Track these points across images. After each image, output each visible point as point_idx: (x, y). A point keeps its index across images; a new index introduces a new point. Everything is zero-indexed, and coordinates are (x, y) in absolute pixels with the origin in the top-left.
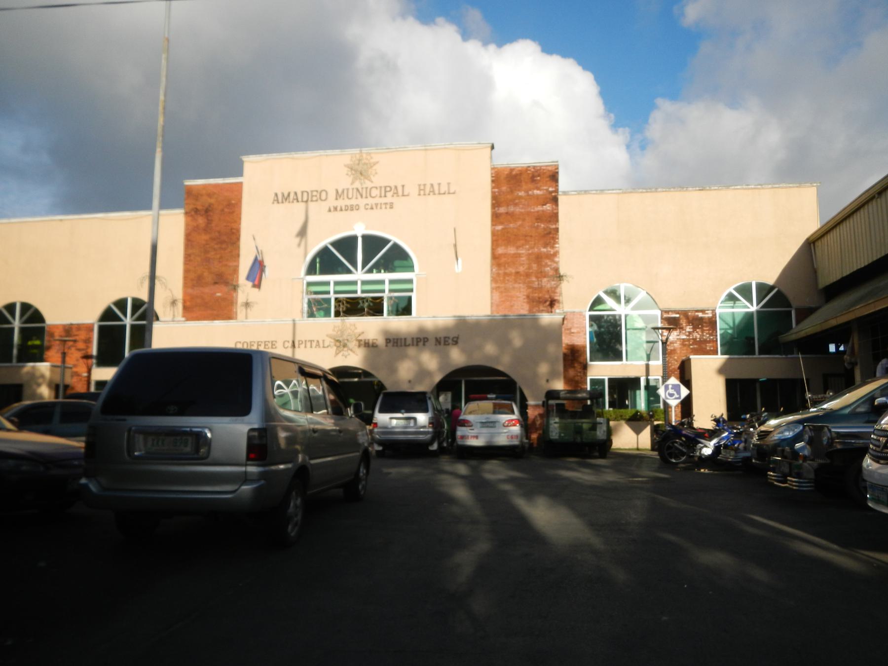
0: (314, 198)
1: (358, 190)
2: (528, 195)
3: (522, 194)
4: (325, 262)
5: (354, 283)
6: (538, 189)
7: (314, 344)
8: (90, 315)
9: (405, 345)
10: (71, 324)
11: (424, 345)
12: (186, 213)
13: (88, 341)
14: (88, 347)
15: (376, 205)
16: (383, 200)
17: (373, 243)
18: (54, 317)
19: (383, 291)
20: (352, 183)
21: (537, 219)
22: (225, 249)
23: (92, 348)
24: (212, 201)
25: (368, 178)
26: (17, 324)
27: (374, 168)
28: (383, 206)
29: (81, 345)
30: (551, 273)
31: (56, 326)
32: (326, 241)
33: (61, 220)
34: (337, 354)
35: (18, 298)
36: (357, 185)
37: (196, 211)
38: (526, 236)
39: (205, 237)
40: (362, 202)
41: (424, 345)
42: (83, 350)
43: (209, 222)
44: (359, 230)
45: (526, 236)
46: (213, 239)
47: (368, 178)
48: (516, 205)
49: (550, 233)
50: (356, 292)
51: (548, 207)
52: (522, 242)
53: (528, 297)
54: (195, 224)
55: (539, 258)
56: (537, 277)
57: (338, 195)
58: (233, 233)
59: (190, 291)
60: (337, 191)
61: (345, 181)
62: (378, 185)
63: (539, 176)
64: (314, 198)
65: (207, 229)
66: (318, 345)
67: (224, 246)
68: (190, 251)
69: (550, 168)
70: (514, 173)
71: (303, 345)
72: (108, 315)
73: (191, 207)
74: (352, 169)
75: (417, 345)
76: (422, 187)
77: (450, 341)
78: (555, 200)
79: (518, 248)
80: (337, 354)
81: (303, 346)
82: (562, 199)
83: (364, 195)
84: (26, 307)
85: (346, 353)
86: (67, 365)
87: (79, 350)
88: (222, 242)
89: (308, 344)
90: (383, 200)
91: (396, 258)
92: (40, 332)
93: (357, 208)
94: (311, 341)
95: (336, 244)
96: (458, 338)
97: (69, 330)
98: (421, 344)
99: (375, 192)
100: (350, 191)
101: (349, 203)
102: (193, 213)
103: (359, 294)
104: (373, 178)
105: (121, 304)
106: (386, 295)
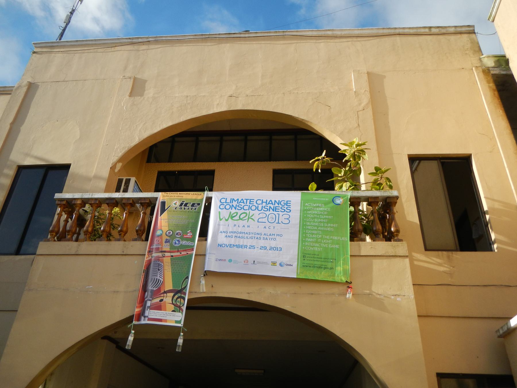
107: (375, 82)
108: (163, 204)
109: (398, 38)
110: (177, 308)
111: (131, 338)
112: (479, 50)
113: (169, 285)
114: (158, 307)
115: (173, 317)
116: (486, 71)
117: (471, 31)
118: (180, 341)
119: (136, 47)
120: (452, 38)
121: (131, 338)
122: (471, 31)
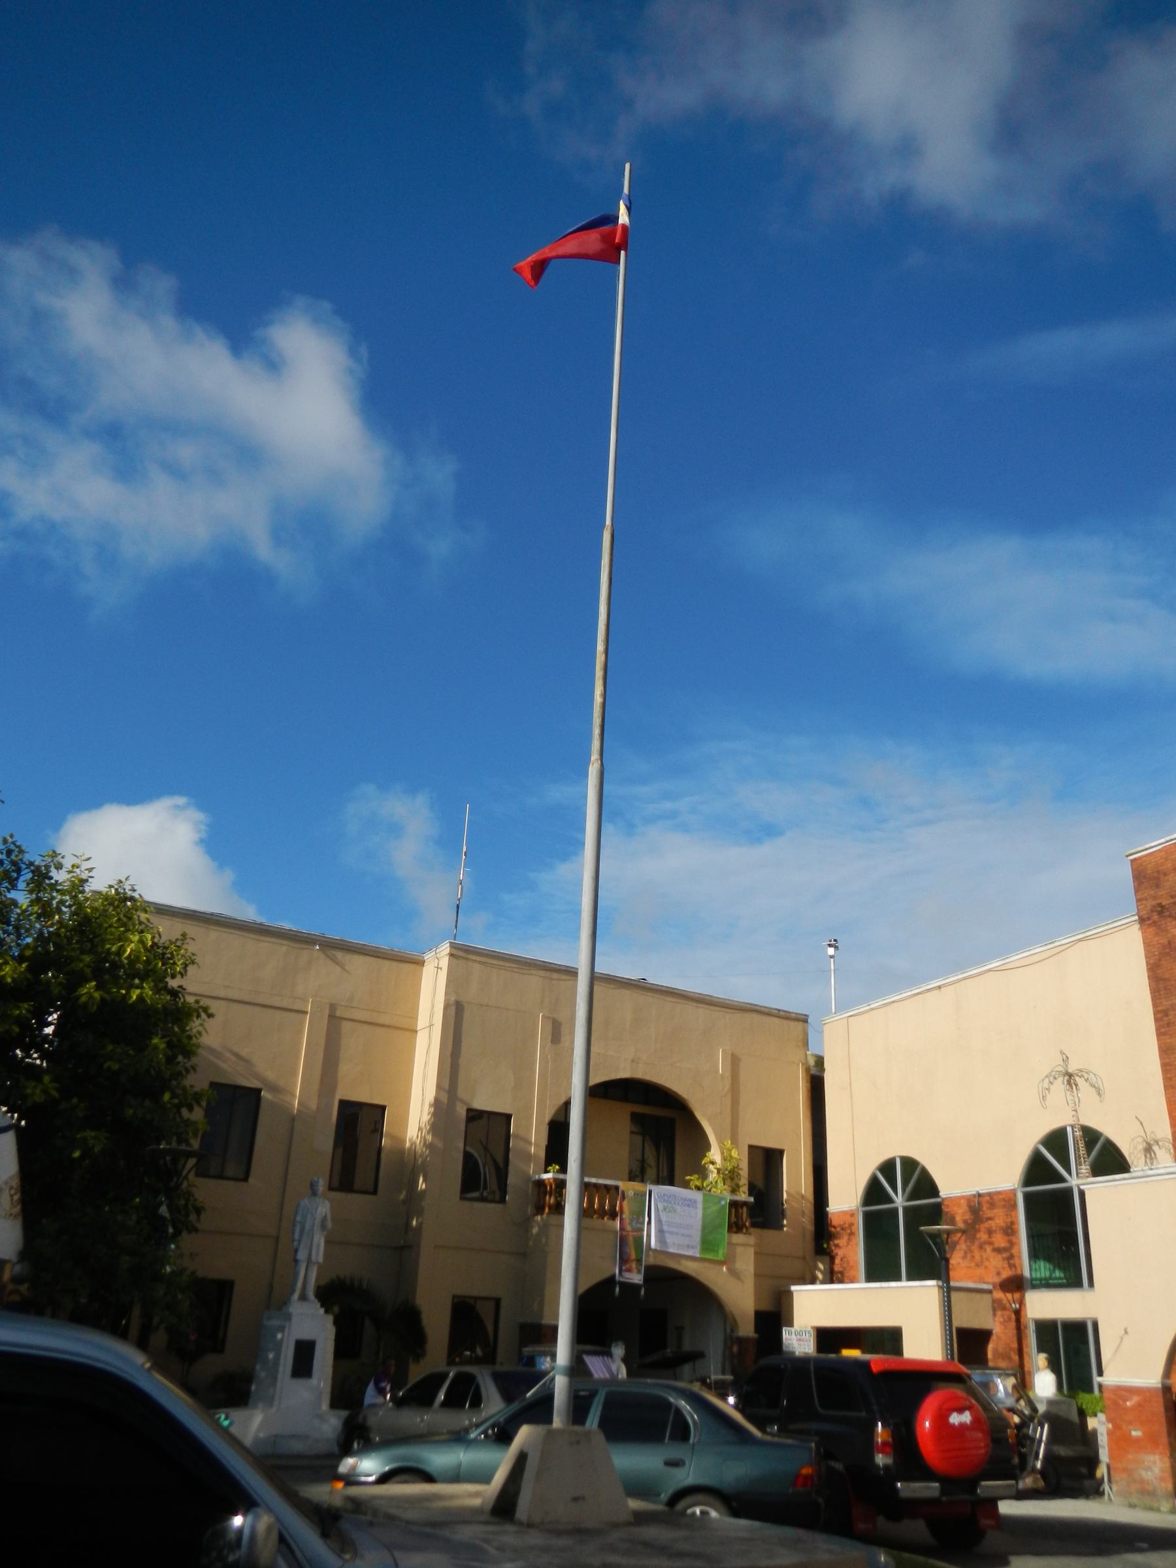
8: (1007, 1175)
10: (980, 1195)
12: (1142, 920)
13: (1010, 1230)
14: (1012, 1244)
18: (952, 1185)
23: (1019, 1244)
26: (899, 1201)
29: (1000, 1240)
31: (955, 1200)
33: (939, 987)
35: (896, 1150)
37: (1161, 910)
42: (1005, 1250)
54: (1164, 941)
68: (1166, 1004)
72: (1037, 1170)
73: (1150, 903)
84: (910, 1164)
86: (952, 1284)
87: (998, 1250)
92: (936, 1213)
97: (979, 1205)
102: (1156, 917)
105: (1056, 1141)
107: (735, 1062)
108: (623, 1193)
109: (755, 1016)
110: (639, 1272)
111: (617, 1290)
112: (806, 1044)
113: (633, 1256)
114: (629, 1270)
115: (637, 1278)
116: (807, 1070)
117: (806, 1021)
118: (643, 1292)
119: (548, 974)
120: (793, 1024)
121: (617, 1290)
122: (804, 1019)
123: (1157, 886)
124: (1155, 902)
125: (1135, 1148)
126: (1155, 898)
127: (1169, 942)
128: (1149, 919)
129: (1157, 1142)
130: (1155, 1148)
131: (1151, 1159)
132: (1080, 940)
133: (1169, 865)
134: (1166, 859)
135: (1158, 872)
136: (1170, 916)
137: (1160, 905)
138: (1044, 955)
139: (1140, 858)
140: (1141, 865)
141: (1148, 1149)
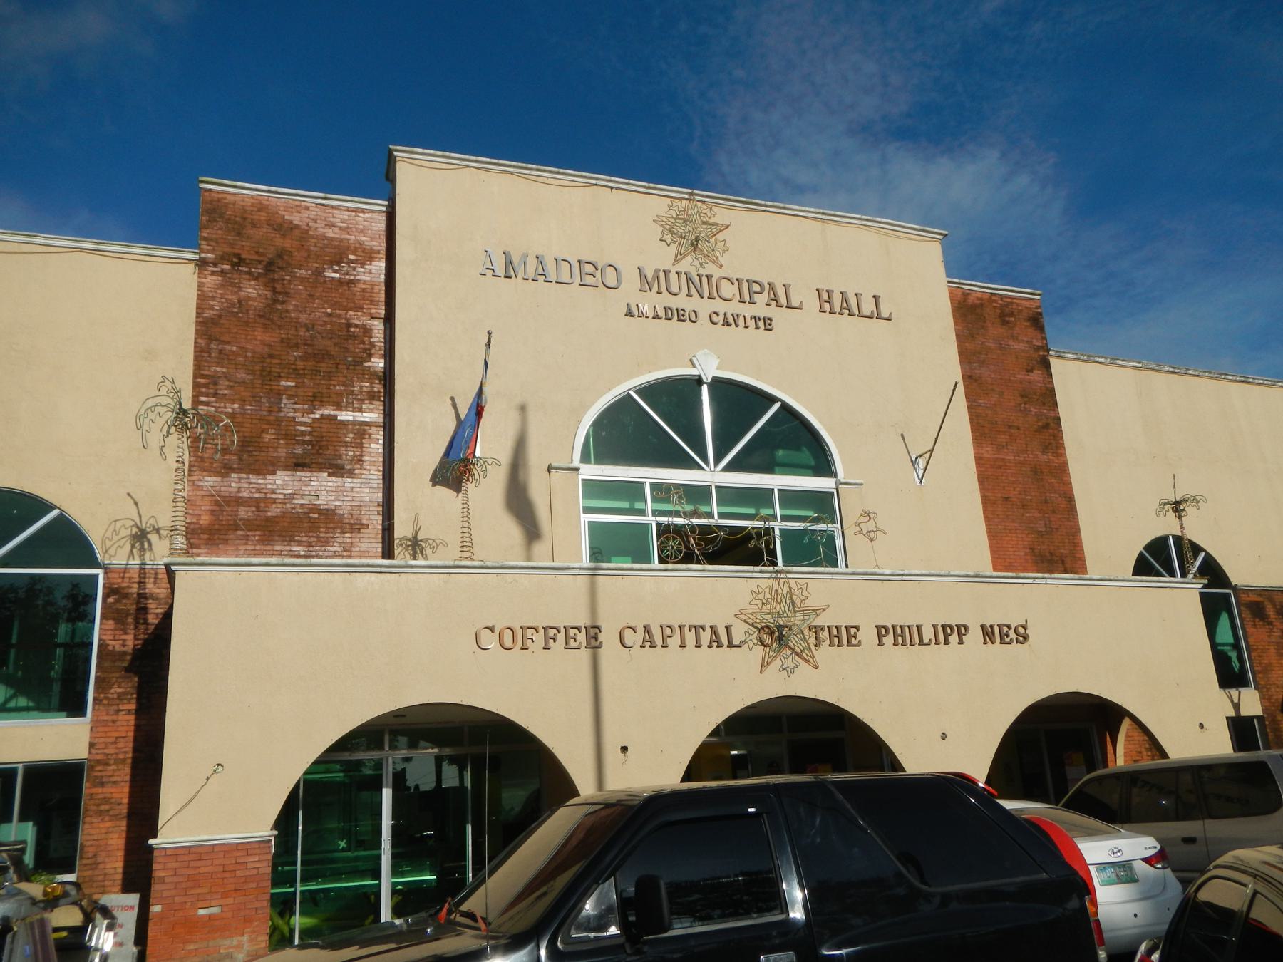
0: (589, 280)
1: (689, 280)
2: (1001, 348)
3: (991, 344)
4: (631, 431)
5: (698, 494)
6: (1014, 338)
7: (705, 637)
9: (921, 643)
11: (961, 642)
15: (736, 317)
16: (748, 310)
17: (739, 402)
19: (773, 517)
20: (676, 261)
21: (1022, 396)
22: (329, 376)
24: (287, 243)
25: (709, 256)
27: (720, 237)
28: (751, 323)
30: (1063, 505)
32: (628, 385)
34: (764, 665)
36: (687, 265)
37: (238, 261)
38: (1010, 427)
39: (259, 339)
40: (705, 307)
41: (961, 642)
43: (278, 294)
44: (709, 368)
45: (1010, 427)
46: (290, 344)
47: (709, 256)
48: (982, 363)
49: (1047, 426)
50: (709, 515)
51: (1037, 375)
52: (1003, 439)
53: (1032, 549)
55: (1037, 472)
56: (1040, 511)
57: (646, 283)
58: (354, 337)
59: (209, 481)
60: (643, 277)
61: (661, 256)
62: (734, 276)
63: (1012, 314)
64: (589, 280)
65: (270, 315)
66: (715, 640)
67: (323, 367)
69: (1027, 304)
70: (971, 300)
71: (674, 641)
74: (672, 233)
75: (947, 642)
76: (826, 297)
77: (1012, 635)
78: (1046, 366)
79: (1000, 448)
80: (764, 665)
81: (674, 641)
82: (1053, 361)
83: (706, 294)
85: (789, 664)
88: (320, 356)
89: (690, 637)
90: (748, 310)
91: (795, 441)
93: (693, 318)
94: (698, 629)
95: (645, 391)
96: (1025, 628)
98: (954, 638)
99: (728, 290)
100: (673, 277)
101: (675, 303)
103: (716, 521)
104: (721, 260)
106: (777, 526)
123: (239, 234)
124: (227, 250)
125: (116, 532)
126: (232, 245)
127: (240, 302)
128: (215, 265)
129: (158, 531)
130: (153, 537)
131: (142, 549)
132: (82, 250)
133: (263, 216)
134: (259, 210)
135: (245, 219)
136: (250, 273)
137: (238, 256)
138: (15, 247)
139: (218, 192)
140: (219, 200)
141: (140, 538)
